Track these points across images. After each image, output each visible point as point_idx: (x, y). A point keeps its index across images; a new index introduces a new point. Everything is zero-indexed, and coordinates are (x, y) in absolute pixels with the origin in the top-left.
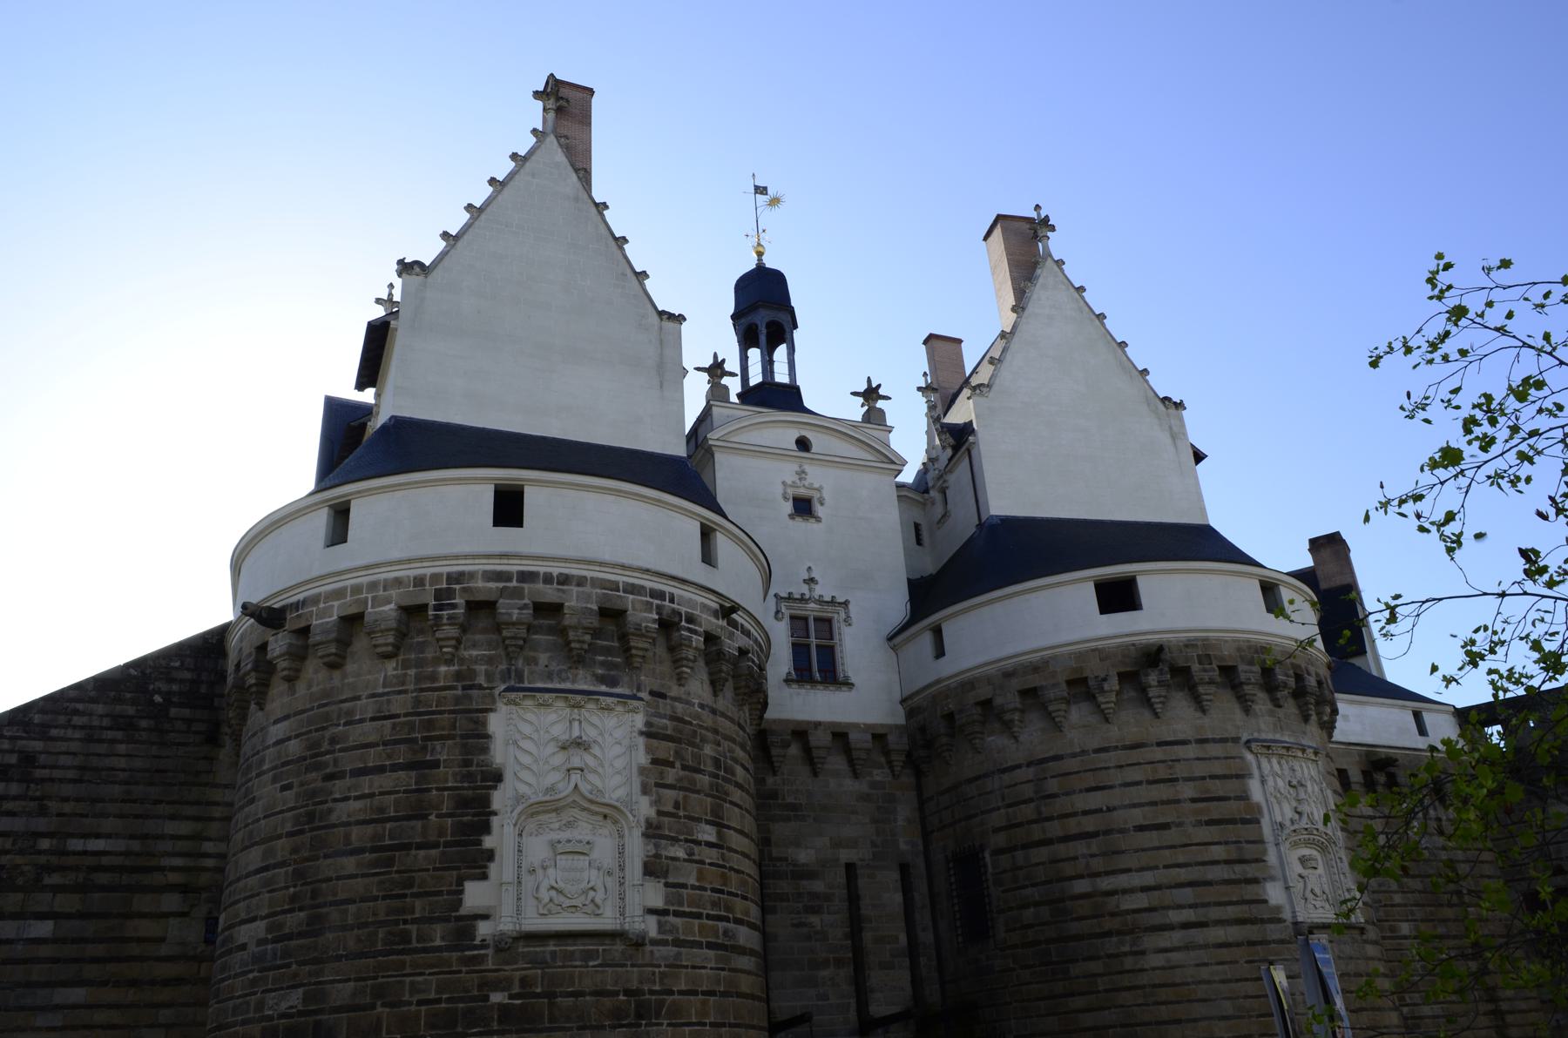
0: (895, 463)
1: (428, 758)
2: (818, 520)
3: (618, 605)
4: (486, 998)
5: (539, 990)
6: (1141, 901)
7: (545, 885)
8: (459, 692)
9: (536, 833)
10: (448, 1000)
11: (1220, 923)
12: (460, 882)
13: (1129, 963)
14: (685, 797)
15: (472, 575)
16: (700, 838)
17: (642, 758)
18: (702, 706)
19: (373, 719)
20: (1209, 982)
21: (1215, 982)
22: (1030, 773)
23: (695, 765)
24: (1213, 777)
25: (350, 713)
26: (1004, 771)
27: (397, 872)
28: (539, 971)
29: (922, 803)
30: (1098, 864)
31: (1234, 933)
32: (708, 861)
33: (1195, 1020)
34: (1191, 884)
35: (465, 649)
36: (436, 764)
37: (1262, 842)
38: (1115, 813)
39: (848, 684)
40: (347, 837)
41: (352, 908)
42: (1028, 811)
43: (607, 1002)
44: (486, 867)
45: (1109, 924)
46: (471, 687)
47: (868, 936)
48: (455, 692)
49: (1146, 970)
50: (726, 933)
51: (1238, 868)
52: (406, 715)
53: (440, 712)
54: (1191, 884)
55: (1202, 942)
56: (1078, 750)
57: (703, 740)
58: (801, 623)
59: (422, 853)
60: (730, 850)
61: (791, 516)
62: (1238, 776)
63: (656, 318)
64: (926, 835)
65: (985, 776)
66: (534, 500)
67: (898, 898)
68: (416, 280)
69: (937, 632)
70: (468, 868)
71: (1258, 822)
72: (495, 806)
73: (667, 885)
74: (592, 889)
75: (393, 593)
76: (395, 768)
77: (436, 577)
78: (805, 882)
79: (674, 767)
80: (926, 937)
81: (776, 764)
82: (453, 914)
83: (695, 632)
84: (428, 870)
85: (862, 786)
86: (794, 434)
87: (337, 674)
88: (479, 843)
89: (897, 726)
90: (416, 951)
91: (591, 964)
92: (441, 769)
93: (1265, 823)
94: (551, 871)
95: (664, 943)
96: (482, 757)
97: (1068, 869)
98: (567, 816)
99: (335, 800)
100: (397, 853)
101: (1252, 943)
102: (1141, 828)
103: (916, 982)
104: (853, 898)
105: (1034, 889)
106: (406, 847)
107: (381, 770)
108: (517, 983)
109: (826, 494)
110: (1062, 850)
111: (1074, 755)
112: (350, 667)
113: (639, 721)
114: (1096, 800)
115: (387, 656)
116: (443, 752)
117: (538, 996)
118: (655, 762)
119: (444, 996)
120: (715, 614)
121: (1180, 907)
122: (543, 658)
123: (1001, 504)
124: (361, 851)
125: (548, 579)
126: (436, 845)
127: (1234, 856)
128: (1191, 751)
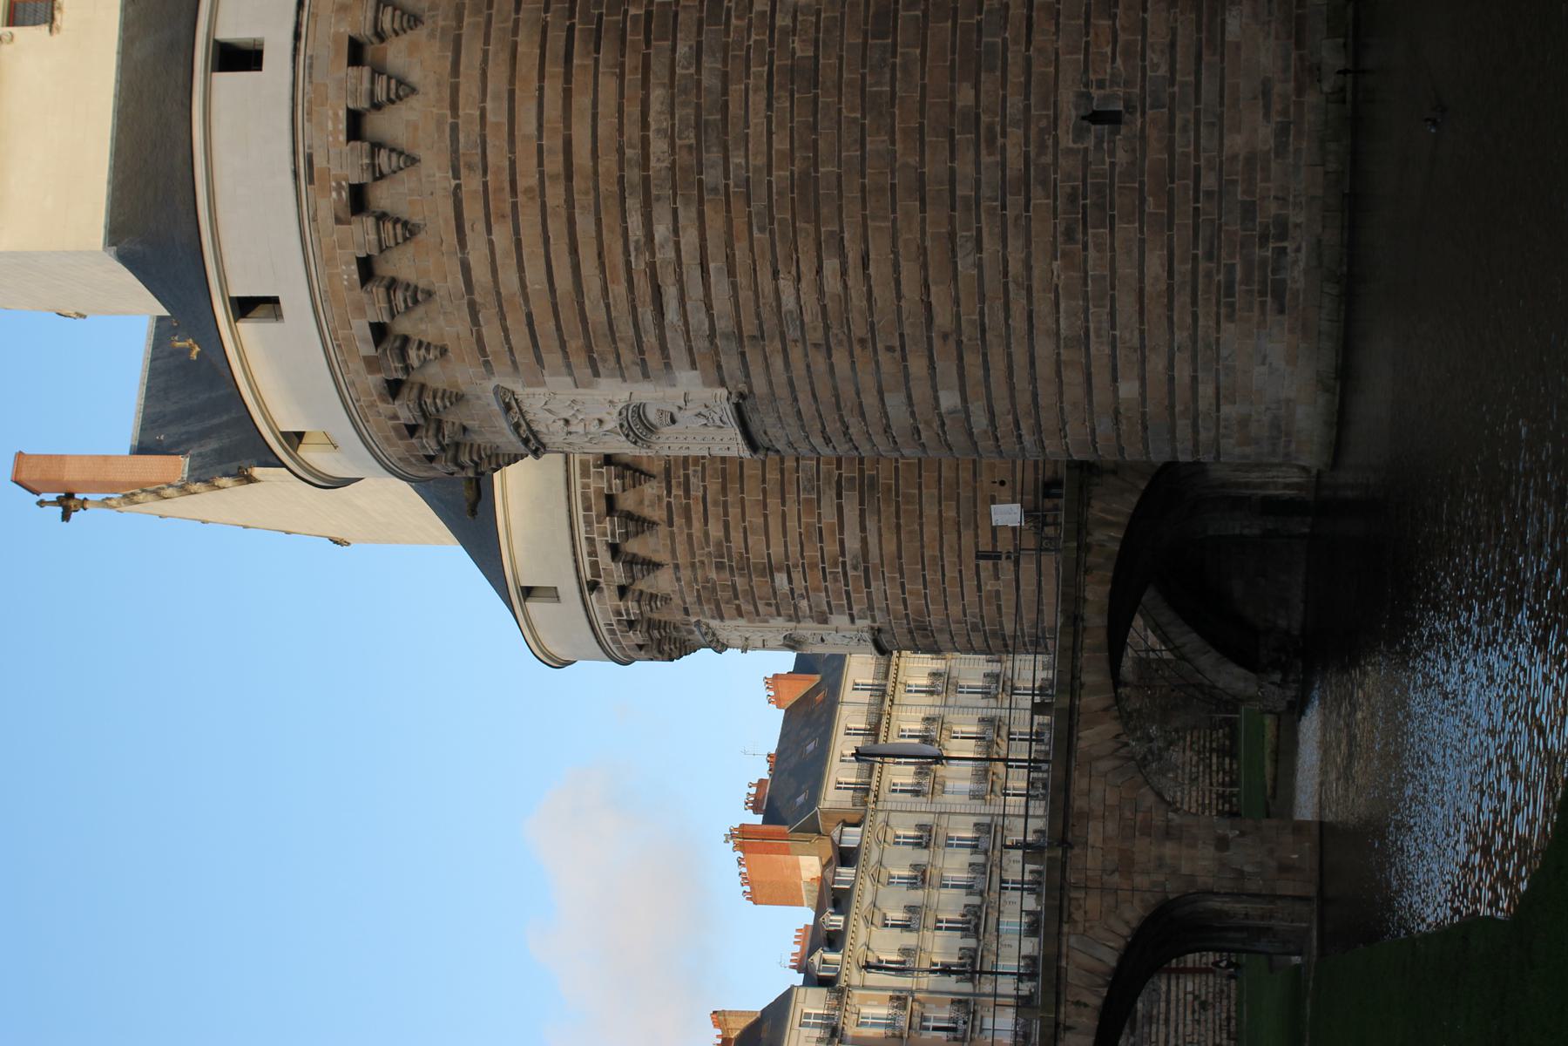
14: (760, 598)
18: (678, 580)
23: (730, 589)
73: (831, 613)
113: (715, 623)
120: (601, 590)
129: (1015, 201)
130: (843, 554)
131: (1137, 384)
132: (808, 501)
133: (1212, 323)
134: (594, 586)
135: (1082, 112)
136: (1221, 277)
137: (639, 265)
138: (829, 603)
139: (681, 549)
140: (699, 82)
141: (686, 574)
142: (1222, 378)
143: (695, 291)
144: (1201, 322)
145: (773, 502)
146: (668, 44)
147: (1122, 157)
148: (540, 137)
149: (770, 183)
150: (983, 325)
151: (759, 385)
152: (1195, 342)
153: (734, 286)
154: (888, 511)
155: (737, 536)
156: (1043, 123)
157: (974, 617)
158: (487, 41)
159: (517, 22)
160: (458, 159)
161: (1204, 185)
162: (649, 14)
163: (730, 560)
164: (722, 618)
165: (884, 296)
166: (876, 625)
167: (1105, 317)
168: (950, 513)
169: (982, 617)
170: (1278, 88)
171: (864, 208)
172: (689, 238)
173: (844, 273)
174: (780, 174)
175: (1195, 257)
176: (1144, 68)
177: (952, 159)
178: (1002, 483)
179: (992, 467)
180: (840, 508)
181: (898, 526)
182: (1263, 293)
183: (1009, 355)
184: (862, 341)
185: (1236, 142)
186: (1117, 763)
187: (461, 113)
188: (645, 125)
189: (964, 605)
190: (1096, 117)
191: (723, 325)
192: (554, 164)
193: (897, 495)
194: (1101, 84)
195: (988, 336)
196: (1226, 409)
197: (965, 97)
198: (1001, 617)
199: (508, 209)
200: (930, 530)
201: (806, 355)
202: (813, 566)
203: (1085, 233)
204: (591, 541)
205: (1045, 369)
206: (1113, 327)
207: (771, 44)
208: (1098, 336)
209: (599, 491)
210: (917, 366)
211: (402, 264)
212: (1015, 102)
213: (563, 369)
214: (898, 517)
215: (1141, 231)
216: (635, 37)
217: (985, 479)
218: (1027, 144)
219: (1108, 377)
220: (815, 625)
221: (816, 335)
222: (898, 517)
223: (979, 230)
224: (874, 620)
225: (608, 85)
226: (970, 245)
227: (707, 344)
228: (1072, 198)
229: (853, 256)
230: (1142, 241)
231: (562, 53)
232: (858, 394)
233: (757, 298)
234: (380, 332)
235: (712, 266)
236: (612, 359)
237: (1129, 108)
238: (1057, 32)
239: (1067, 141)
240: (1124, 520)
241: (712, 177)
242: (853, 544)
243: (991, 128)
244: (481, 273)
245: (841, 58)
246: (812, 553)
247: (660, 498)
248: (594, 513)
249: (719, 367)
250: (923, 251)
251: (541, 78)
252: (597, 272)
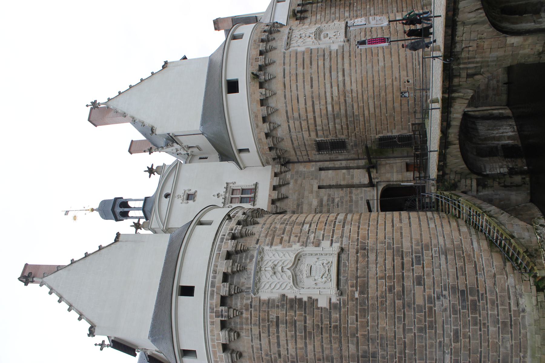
0: (177, 163)
1: (275, 320)
2: (196, 192)
3: (225, 253)
4: (357, 299)
5: (355, 281)
6: (335, 89)
7: (320, 280)
8: (253, 309)
9: (303, 283)
10: (357, 311)
11: (343, 65)
12: (318, 308)
13: (355, 95)
14: (293, 234)
15: (211, 304)
16: (308, 229)
17: (279, 247)
18: (262, 228)
19: (260, 340)
20: (361, 70)
21: (361, 68)
22: (291, 122)
23: (282, 230)
24: (296, 62)
25: (257, 349)
26: (290, 131)
27: (313, 330)
28: (349, 281)
29: (299, 162)
30: (323, 102)
31: (346, 61)
32: (315, 227)
33: (373, 76)
34: (330, 72)
35: (237, 307)
36: (278, 318)
37: (318, 49)
38: (306, 94)
39: (256, 184)
40: (301, 349)
41: (325, 346)
42: (304, 124)
43: (360, 259)
44: (314, 300)
45: (342, 100)
46: (251, 305)
47: (342, 183)
48: (252, 311)
49: (357, 90)
50: (339, 222)
51: (326, 57)
52: (259, 328)
53: (259, 316)
54: (330, 72)
55: (349, 71)
56: (285, 105)
58: (233, 200)
59: (307, 322)
60: (312, 220)
61: (194, 201)
62: (296, 54)
63: (118, 243)
64: (310, 161)
65: (291, 138)
66: (185, 282)
67: (330, 172)
68: (97, 330)
69: (241, 151)
70: (314, 306)
71: (311, 49)
72: (293, 297)
73: (323, 240)
74: (323, 264)
75: (216, 332)
76: (278, 332)
77: (211, 317)
78: (324, 203)
79: (283, 237)
80: (344, 163)
81: (283, 211)
82: (329, 310)
84: (313, 319)
85: (292, 182)
86: (164, 198)
87: (244, 354)
88: (305, 302)
89: (272, 168)
90: (340, 323)
91: (347, 264)
92: (279, 315)
93: (312, 47)
94: (316, 278)
96: (276, 301)
97: (324, 112)
98: (298, 273)
99: (288, 353)
100: (307, 330)
101: (350, 56)
102: (312, 86)
103: (358, 168)
104: (330, 187)
105: (330, 124)
106: (305, 327)
107: (278, 337)
108: (352, 289)
109: (186, 189)
110: (317, 114)
111: (286, 106)
112: (241, 349)
114: (302, 100)
115: (239, 335)
116: (273, 315)
117: (357, 282)
118: (281, 243)
119: (355, 313)
121: (338, 77)
122: (243, 280)
123: (196, 125)
124: (306, 343)
125: (214, 277)
126: (305, 317)
127: (322, 58)
128: (287, 68)
157: (389, 239)
189: (385, 233)
198: (402, 238)
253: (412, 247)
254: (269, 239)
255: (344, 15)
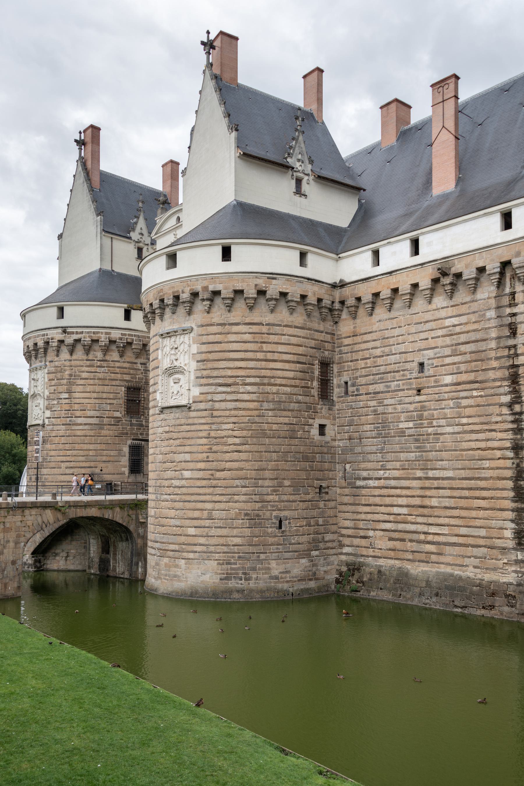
17: (46, 380)
18: (65, 361)
57: (65, 370)
60: (74, 398)
83: (54, 342)
95: (50, 425)
113: (46, 371)
118: (50, 380)
129: (257, 498)
130: (76, 417)
131: (194, 534)
132: (95, 407)
133: (216, 558)
134: (65, 332)
135: (282, 518)
136: (232, 561)
137: (238, 380)
138: (56, 411)
139: (78, 363)
140: (292, 403)
141: (67, 363)
142: (196, 561)
143: (229, 397)
144: (217, 555)
145: (95, 395)
146: (301, 393)
147: (270, 530)
148: (277, 352)
149: (263, 423)
150: (217, 487)
151: (193, 414)
152: (210, 553)
153: (231, 410)
154: (92, 433)
155: (82, 382)
156: (279, 507)
158: (303, 338)
159: (307, 347)
160: (272, 326)
161: (261, 555)
162: (308, 388)
163: (73, 379)
164: (48, 373)
165: (227, 456)
166: (46, 426)
167: (219, 525)
168: (91, 453)
169: (50, 462)
170: (288, 575)
171: (255, 452)
172: (246, 397)
173: (235, 444)
174: (266, 426)
175: (239, 553)
176: (293, 536)
177: (270, 479)
178: (101, 470)
179: (107, 467)
180: (93, 417)
181: (86, 436)
182: (227, 574)
183: (205, 495)
184: (211, 449)
185: (273, 564)
186: (40, 524)
187: (284, 328)
188: (281, 385)
190: (280, 522)
191: (217, 405)
192: (269, 356)
193: (97, 436)
194: (289, 523)
195: (212, 489)
196: (183, 561)
197: (287, 483)
199: (256, 340)
200: (85, 447)
201: (205, 430)
202: (71, 407)
203: (247, 519)
204: (82, 333)
205: (200, 505)
206: (215, 527)
207: (301, 425)
208: (212, 523)
209: (101, 338)
210: (201, 465)
211: (240, 305)
212: (285, 498)
213: (200, 351)
214: (90, 436)
215: (247, 537)
216: (303, 383)
217: (103, 465)
218: (274, 502)
219: (196, 525)
220: (45, 405)
221: (213, 434)
222: (90, 436)
223: (248, 487)
224: (47, 425)
225: (291, 374)
226: (244, 484)
227: (210, 399)
228: (258, 515)
229: (240, 448)
230: (244, 537)
231: (300, 361)
232: (190, 445)
233: (226, 417)
234: (217, 293)
235: (237, 403)
236: (202, 367)
237: (283, 532)
238: (303, 510)
239: (274, 513)
240: (114, 520)
241: (266, 405)
242: (79, 420)
243: (278, 491)
244: (235, 329)
245: (297, 446)
246: (76, 407)
247: (96, 357)
248: (92, 335)
249: (201, 402)
250: (242, 469)
251: (294, 354)
252: (235, 366)
253: (44, 475)
254: (53, 369)
255: (445, 375)
